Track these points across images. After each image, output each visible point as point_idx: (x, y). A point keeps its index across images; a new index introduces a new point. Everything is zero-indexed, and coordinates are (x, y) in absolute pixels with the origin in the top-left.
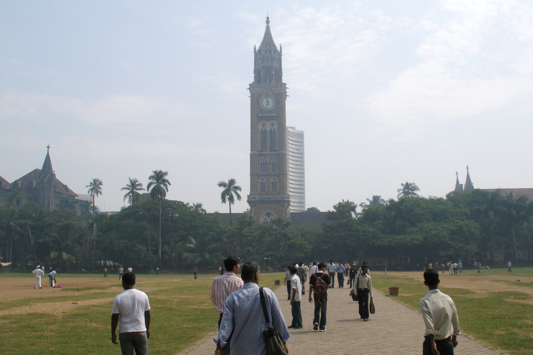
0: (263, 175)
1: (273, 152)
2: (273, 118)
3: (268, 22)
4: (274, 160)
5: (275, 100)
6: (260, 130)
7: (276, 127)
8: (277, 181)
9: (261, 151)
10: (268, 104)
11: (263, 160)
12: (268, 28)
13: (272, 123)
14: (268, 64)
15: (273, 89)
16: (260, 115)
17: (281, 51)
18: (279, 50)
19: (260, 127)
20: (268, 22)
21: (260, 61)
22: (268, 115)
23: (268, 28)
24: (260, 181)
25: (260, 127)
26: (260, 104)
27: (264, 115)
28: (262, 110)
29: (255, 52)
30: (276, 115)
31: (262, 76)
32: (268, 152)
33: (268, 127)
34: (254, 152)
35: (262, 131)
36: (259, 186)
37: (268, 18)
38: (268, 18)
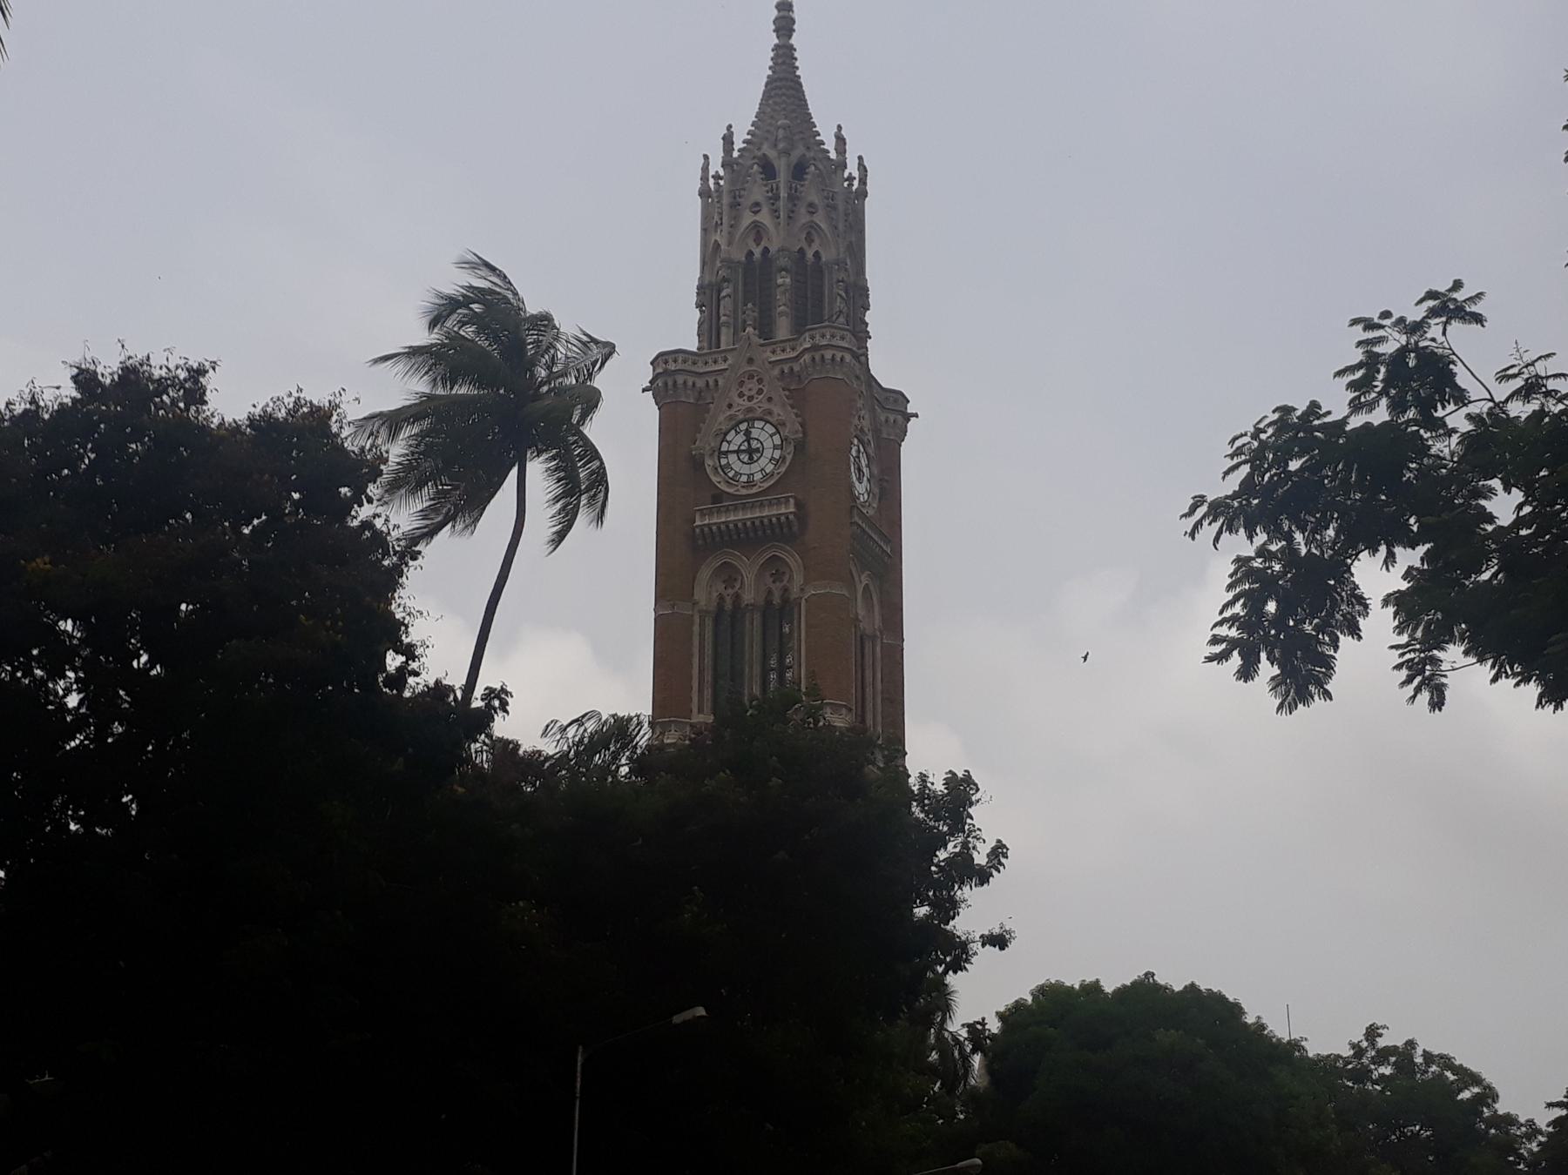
3: (785, 26)
6: (713, 607)
12: (784, 57)
20: (785, 26)
23: (784, 57)
25: (706, 592)
28: (718, 497)
29: (704, 193)
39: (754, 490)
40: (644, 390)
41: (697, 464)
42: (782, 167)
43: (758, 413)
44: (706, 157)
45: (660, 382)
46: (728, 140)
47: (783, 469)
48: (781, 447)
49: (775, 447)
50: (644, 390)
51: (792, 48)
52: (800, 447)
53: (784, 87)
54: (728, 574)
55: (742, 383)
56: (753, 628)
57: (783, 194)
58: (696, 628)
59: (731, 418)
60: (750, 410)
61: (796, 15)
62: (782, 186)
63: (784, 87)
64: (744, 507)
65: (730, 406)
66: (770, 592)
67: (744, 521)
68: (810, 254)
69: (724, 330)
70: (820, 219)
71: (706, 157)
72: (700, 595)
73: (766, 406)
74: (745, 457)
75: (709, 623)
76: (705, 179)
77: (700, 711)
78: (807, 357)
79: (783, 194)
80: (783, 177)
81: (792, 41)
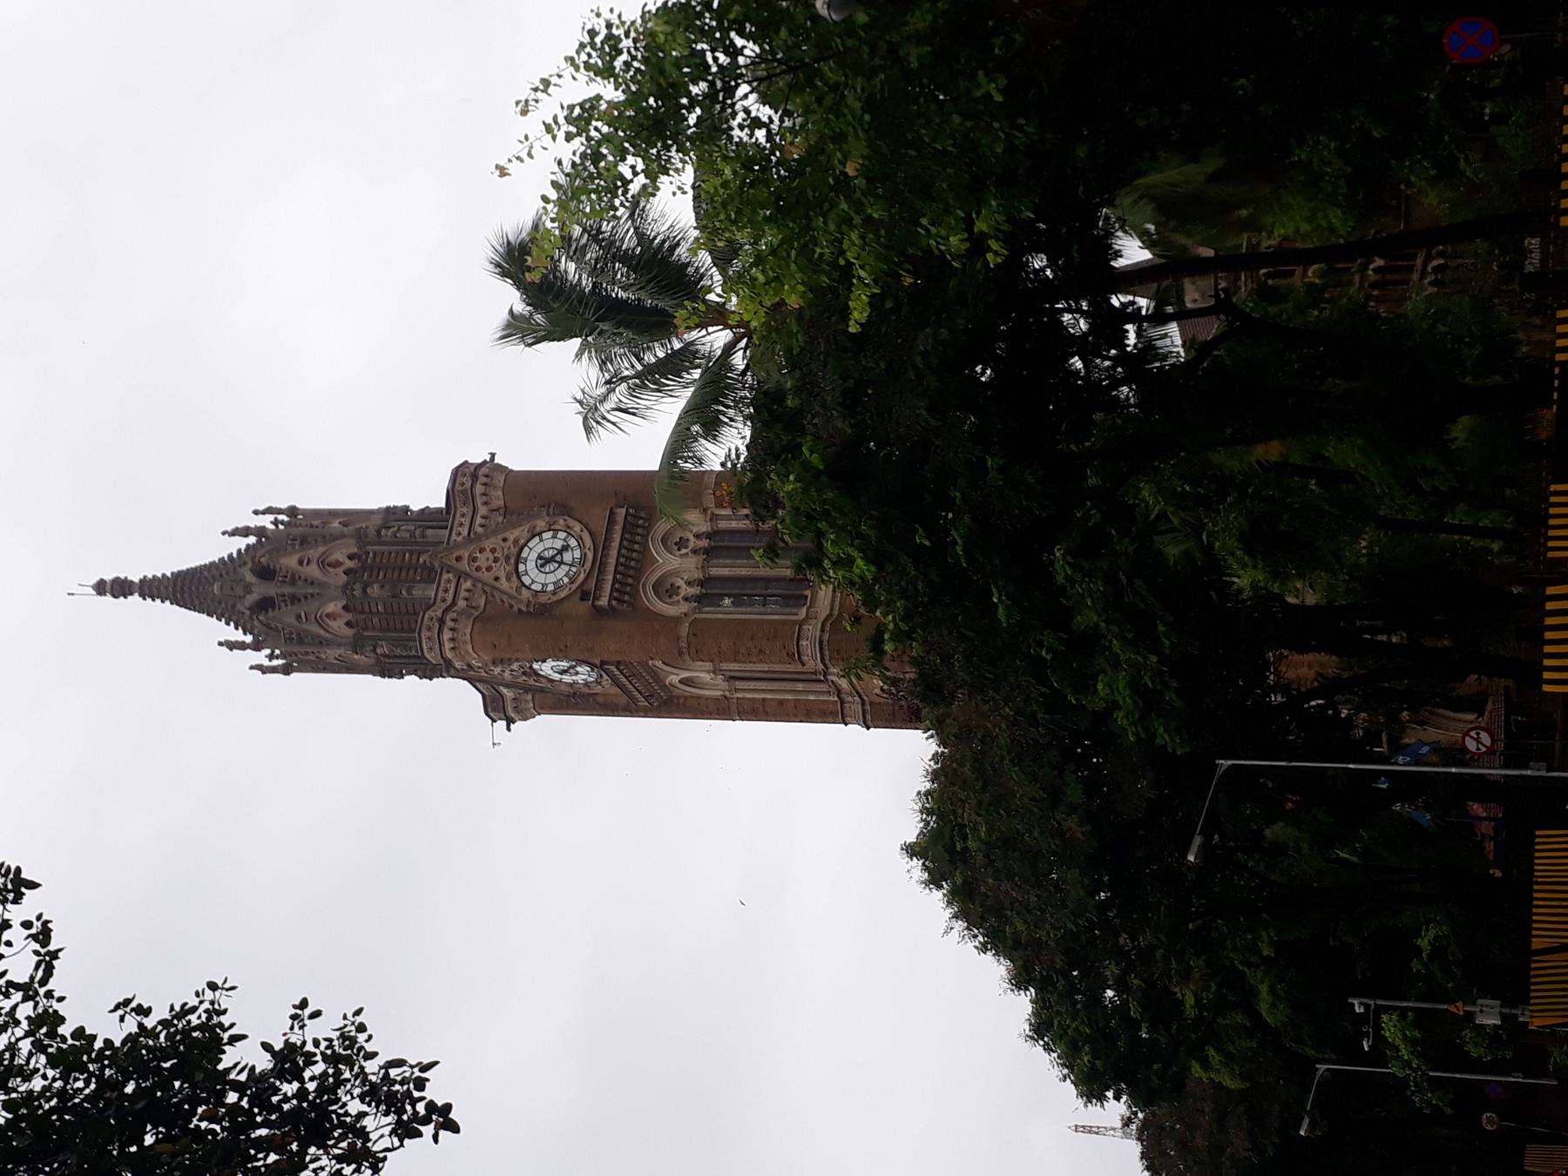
12: (152, 589)
14: (337, 564)
15: (480, 530)
22: (614, 553)
23: (152, 589)
37: (101, 588)
38: (101, 588)
39: (590, 556)
42: (261, 590)
43: (514, 551)
48: (556, 531)
49: (554, 537)
51: (144, 581)
54: (665, 589)
55: (478, 569)
57: (288, 590)
59: (508, 579)
60: (507, 558)
61: (108, 577)
62: (279, 591)
65: (497, 579)
71: (220, 644)
73: (510, 542)
79: (288, 590)
80: (271, 590)
81: (136, 580)
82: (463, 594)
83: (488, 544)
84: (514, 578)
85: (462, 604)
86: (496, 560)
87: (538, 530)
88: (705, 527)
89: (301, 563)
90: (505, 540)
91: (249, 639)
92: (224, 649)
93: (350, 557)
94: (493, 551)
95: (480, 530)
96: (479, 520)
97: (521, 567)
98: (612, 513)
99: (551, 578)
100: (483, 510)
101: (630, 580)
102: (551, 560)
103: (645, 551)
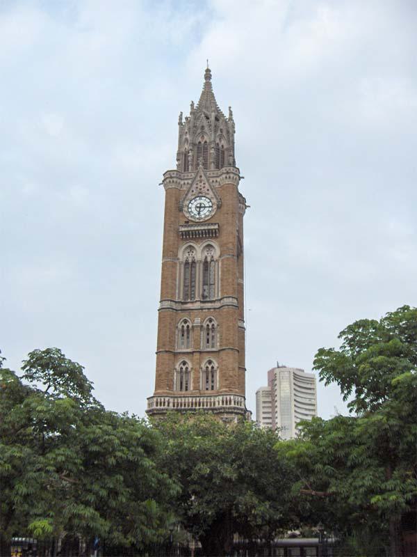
0: (184, 353)
1: (209, 305)
2: (212, 234)
3: (208, 75)
4: (211, 321)
5: (214, 201)
7: (216, 253)
8: (216, 365)
9: (183, 303)
10: (200, 208)
11: (186, 321)
12: (208, 85)
13: (209, 246)
15: (211, 181)
16: (183, 229)
17: (231, 119)
18: (227, 115)
19: (182, 255)
20: (208, 75)
21: (188, 136)
23: (208, 85)
24: (178, 367)
25: (182, 255)
26: (186, 209)
27: (192, 228)
29: (180, 124)
30: (216, 227)
31: (190, 159)
32: (197, 305)
33: (199, 254)
34: (167, 304)
35: (187, 263)
36: (176, 377)
37: (208, 71)
38: (208, 71)
39: (201, 221)
40: (160, 184)
41: (181, 210)
43: (204, 195)
44: (182, 113)
45: (168, 181)
46: (192, 105)
47: (213, 214)
50: (160, 184)
52: (219, 207)
53: (208, 94)
55: (197, 184)
56: (199, 270)
58: (178, 267)
63: (208, 94)
64: (199, 225)
66: (206, 257)
67: (202, 230)
68: (220, 146)
69: (190, 167)
70: (224, 133)
71: (182, 113)
72: (180, 255)
73: (207, 192)
74: (202, 209)
75: (183, 266)
76: (181, 118)
77: (179, 298)
78: (224, 176)
82: (186, 182)
83: (207, 185)
84: (193, 197)
85: (182, 182)
86: (201, 189)
87: (212, 200)
88: (216, 257)
89: (221, 130)
90: (208, 190)
91: (184, 120)
92: (179, 114)
93: (206, 142)
94: (204, 187)
95: (211, 181)
96: (214, 179)
97: (198, 199)
98: (215, 224)
99: (193, 209)
100: (218, 179)
101: (191, 236)
102: (200, 207)
103: (202, 238)
